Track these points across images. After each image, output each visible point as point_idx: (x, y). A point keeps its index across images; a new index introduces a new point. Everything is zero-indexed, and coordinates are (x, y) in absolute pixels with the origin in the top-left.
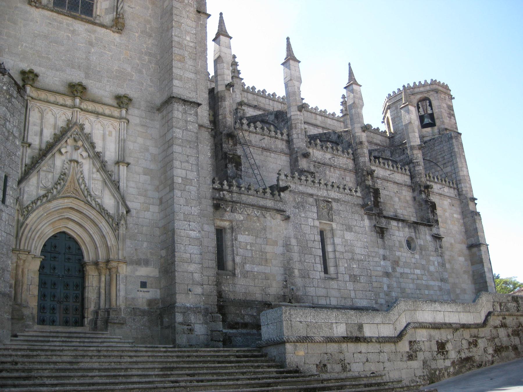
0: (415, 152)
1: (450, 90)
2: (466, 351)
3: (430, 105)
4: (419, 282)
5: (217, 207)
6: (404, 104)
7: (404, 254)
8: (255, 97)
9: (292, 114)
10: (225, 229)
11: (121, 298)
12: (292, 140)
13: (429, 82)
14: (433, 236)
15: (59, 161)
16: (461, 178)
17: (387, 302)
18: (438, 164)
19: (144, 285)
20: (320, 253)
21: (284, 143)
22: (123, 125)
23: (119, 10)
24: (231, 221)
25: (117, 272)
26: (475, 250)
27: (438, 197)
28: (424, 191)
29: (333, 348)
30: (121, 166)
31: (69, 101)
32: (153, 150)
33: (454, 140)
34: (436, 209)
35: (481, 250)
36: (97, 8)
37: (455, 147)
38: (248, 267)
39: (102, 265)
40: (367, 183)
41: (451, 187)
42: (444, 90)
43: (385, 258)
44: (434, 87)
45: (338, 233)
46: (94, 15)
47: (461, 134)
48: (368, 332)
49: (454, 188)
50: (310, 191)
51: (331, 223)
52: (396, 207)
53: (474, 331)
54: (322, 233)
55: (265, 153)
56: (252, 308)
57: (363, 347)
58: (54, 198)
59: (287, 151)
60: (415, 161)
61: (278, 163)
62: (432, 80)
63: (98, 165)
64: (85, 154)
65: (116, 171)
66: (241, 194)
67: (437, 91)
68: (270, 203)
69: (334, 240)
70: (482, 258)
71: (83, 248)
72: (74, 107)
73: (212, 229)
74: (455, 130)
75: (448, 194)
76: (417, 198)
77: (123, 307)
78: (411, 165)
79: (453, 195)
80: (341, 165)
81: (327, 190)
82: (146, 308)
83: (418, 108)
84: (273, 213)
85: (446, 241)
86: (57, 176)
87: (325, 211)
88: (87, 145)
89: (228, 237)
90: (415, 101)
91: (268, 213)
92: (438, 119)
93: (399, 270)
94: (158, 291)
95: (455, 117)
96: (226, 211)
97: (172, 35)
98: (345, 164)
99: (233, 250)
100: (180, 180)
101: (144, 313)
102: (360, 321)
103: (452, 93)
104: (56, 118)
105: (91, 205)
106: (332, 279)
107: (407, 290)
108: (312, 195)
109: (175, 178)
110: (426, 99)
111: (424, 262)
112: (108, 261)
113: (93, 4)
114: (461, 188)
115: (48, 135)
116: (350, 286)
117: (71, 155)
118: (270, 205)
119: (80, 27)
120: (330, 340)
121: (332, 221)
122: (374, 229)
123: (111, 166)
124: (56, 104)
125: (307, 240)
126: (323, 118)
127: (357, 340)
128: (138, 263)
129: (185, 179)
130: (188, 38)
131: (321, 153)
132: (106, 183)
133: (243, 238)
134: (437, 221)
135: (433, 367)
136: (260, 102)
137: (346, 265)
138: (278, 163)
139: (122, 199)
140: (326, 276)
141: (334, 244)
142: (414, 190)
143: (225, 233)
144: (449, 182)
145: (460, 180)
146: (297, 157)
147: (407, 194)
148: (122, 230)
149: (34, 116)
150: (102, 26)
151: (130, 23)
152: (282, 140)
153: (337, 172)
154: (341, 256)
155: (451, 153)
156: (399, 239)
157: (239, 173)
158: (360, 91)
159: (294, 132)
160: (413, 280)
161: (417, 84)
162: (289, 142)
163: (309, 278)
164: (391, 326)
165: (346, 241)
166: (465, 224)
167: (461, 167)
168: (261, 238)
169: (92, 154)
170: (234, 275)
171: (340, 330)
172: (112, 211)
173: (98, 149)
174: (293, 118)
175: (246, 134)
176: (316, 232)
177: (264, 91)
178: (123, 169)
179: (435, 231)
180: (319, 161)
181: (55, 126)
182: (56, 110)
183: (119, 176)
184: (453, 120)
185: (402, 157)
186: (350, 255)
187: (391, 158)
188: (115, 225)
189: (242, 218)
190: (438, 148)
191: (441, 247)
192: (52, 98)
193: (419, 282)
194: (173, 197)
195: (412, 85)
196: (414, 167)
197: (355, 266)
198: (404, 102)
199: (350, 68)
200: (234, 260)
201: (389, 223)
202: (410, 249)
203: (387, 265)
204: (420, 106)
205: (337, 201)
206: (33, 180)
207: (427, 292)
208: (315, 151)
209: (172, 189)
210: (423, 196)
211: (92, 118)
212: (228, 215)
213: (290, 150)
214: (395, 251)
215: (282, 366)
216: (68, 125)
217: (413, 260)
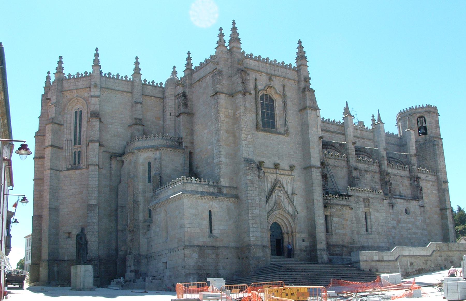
0: (413, 158)
1: (438, 110)
2: (422, 266)
3: (425, 121)
4: (410, 231)
6: (408, 129)
7: (404, 217)
8: (324, 124)
9: (349, 146)
10: (328, 215)
11: (297, 246)
12: (349, 161)
13: (425, 106)
14: (419, 206)
15: (274, 195)
16: (439, 170)
17: (393, 241)
18: (427, 159)
19: (303, 241)
21: (345, 162)
23: (287, 125)
24: (331, 213)
25: (295, 236)
26: (443, 211)
27: (424, 182)
28: (416, 181)
29: (374, 264)
30: (294, 196)
32: (303, 187)
33: (436, 147)
34: (422, 190)
35: (447, 212)
36: (277, 124)
37: (437, 150)
38: (337, 231)
39: (290, 234)
40: (386, 180)
41: (433, 175)
42: (434, 110)
43: (393, 219)
44: (428, 109)
45: (372, 213)
46: (276, 128)
47: (442, 139)
48: (385, 258)
49: (435, 176)
50: (360, 195)
51: (369, 209)
52: (401, 190)
53: (426, 258)
55: (336, 169)
56: (339, 247)
58: (274, 210)
59: (347, 167)
60: (412, 163)
61: (343, 173)
62: (427, 105)
63: (287, 196)
64: (282, 192)
65: (292, 197)
66: (334, 200)
67: (429, 112)
68: (345, 203)
69: (370, 217)
70: (447, 216)
71: (282, 228)
73: (325, 216)
74: (439, 136)
75: (431, 180)
76: (412, 184)
77: (298, 249)
78: (410, 165)
79: (434, 180)
80: (373, 170)
81: (368, 194)
82: (305, 249)
83: (418, 122)
84: (346, 207)
85: (428, 207)
86: (274, 202)
87: (367, 204)
88: (282, 189)
89: (329, 219)
90: (416, 118)
91: (344, 207)
92: (429, 130)
93: (400, 225)
94: (308, 243)
95: (439, 128)
96: (328, 208)
97: (309, 137)
98: (375, 169)
99: (331, 224)
100: (316, 200)
101: (305, 251)
102: (382, 255)
103: (438, 112)
104: (271, 179)
105: (286, 212)
106: (369, 234)
107: (404, 235)
108: (362, 197)
109: (314, 200)
110: (422, 117)
111: (413, 221)
112: (292, 232)
113: (275, 122)
114: (439, 175)
116: (377, 237)
117: (278, 193)
118: (345, 204)
119: (274, 136)
120: (373, 261)
121: (370, 208)
122: (388, 204)
123: (290, 196)
124: (270, 173)
125: (359, 218)
126: (361, 131)
128: (301, 232)
129: (318, 200)
130: (315, 138)
131: (363, 165)
132: (289, 203)
133: (335, 219)
134: (422, 198)
135: (408, 271)
136: (327, 127)
137: (375, 228)
138: (343, 173)
140: (368, 233)
141: (370, 218)
142: (411, 180)
143: (328, 217)
144: (432, 172)
145: (438, 171)
146: (352, 170)
147: (407, 182)
148: (296, 221)
150: (280, 134)
151: (291, 130)
152: (344, 160)
153: (371, 174)
154: (374, 224)
155: (435, 154)
156: (401, 209)
157: (326, 182)
158: (384, 127)
159: (350, 157)
160: (407, 230)
161: (418, 107)
162: (348, 161)
163: (360, 234)
164: (393, 257)
165: (376, 216)
166: (439, 197)
167: (439, 163)
168: (341, 218)
169: (284, 192)
170: (332, 234)
171: (376, 258)
173: (286, 190)
174: (349, 149)
175: (328, 160)
176: (363, 214)
177: (329, 120)
178: (295, 197)
179: (421, 203)
180: (362, 169)
181: (271, 182)
182: (271, 175)
183: (293, 199)
184: (438, 130)
185: (405, 160)
186: (377, 223)
187: (399, 159)
189: (334, 210)
190: (427, 149)
191: (424, 212)
193: (410, 231)
194: (314, 208)
195: (414, 107)
196: (412, 166)
197: (379, 228)
198: (408, 128)
199: (378, 112)
200: (332, 229)
201: (396, 201)
202: (406, 214)
203: (394, 223)
204: (419, 121)
205: (373, 198)
206: (268, 203)
207: (414, 236)
208: (359, 164)
209: (314, 205)
210: (416, 183)
211: (282, 177)
212: (329, 210)
213: (348, 165)
214: (398, 215)
215: (360, 269)
216: (275, 182)
217: (408, 220)
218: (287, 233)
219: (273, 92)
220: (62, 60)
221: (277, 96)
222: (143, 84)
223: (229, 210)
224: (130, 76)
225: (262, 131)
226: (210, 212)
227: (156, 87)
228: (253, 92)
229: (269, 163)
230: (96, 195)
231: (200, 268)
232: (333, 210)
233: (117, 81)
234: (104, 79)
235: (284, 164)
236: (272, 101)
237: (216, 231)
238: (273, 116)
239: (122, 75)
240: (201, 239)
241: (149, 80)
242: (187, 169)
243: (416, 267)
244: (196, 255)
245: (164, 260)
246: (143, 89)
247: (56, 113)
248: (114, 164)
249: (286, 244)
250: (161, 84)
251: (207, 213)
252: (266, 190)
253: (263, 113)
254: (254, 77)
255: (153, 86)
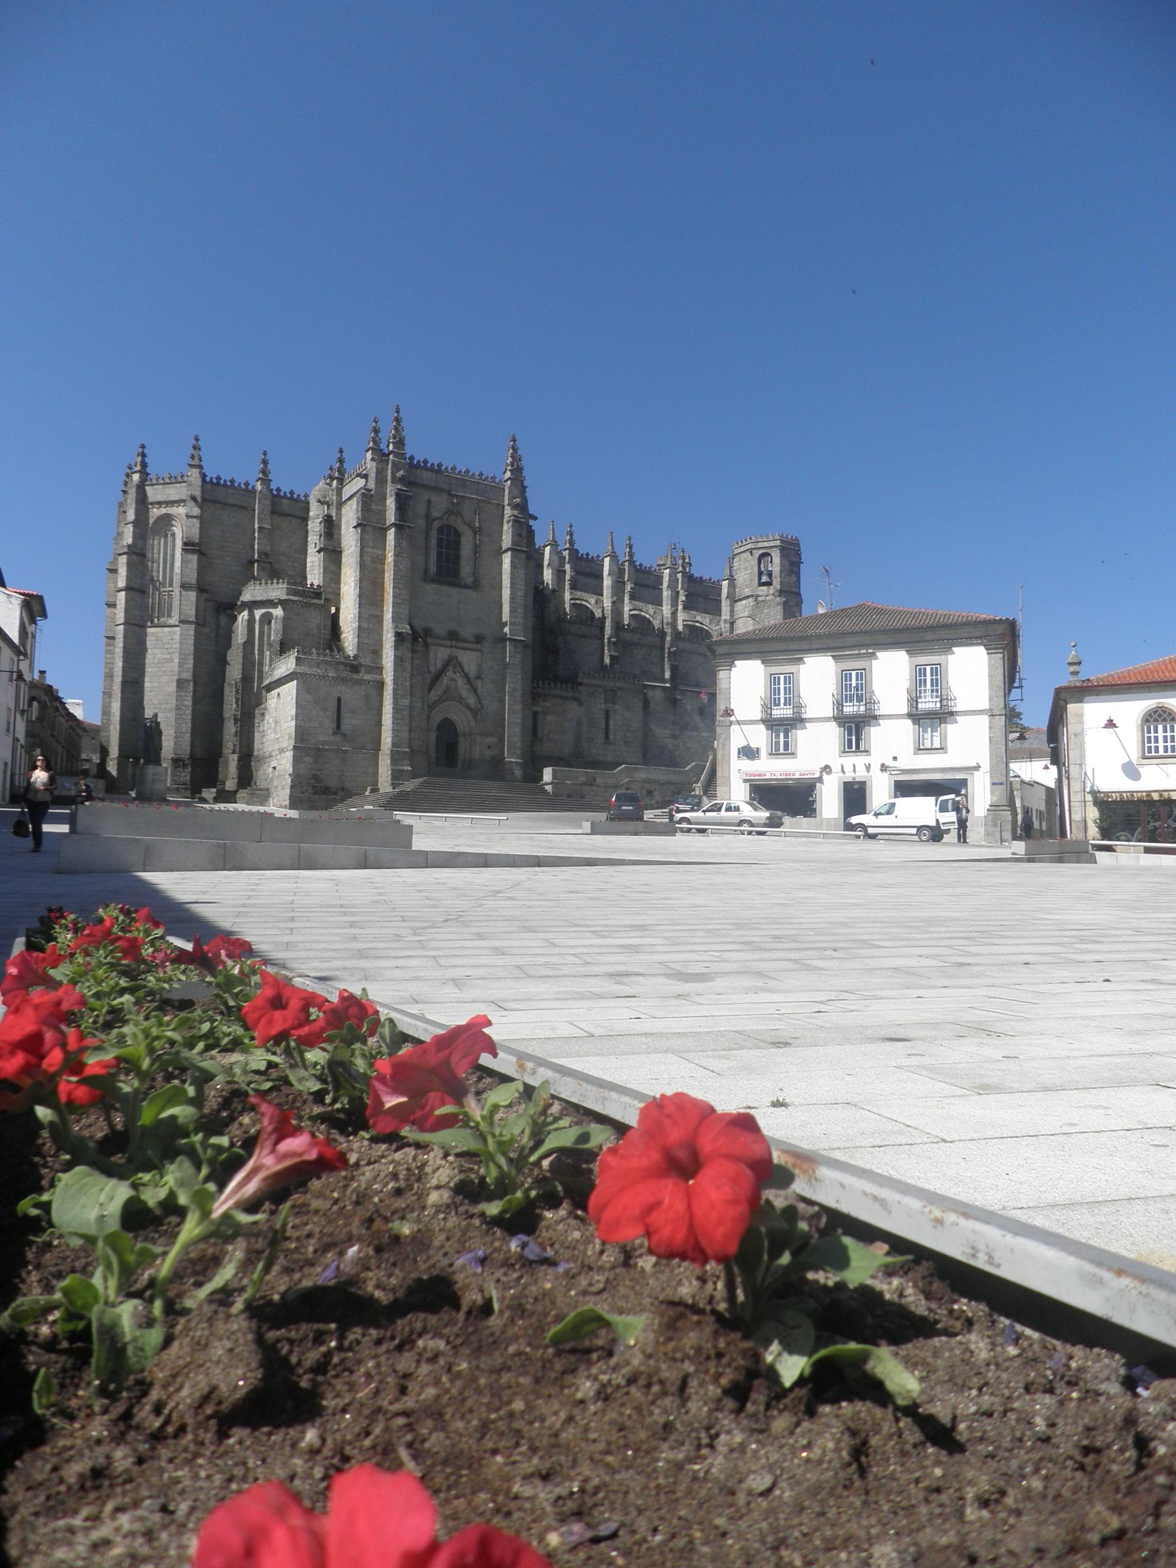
5: (534, 699)
15: (445, 680)
20: (604, 726)
22: (479, 654)
31: (449, 643)
50: (600, 683)
54: (607, 713)
57: (595, 788)
68: (570, 694)
72: (451, 646)
83: (759, 563)
115: (439, 664)
119: (454, 591)
124: (443, 645)
127: (591, 785)
133: (549, 718)
139: (479, 699)
149: (432, 654)
150: (466, 587)
172: (473, 706)
178: (479, 683)
182: (441, 649)
188: (475, 712)
192: (441, 642)
205: (621, 689)
206: (433, 692)
211: (461, 652)
218: (464, 735)
219: (460, 521)
220: (146, 451)
221: (466, 528)
222: (274, 496)
223: (367, 697)
224: (252, 483)
225: (433, 581)
226: (339, 699)
227: (297, 500)
228: (421, 523)
229: (440, 629)
230: (191, 666)
231: (315, 777)
232: (548, 704)
233: (230, 491)
234: (209, 486)
235: (467, 632)
236: (458, 535)
237: (344, 727)
238: (457, 559)
239: (240, 480)
240: (321, 738)
241: (285, 489)
242: (327, 633)
243: (658, 798)
244: (309, 760)
245: (273, 764)
246: (273, 503)
247: (134, 537)
248: (223, 619)
249: (462, 749)
250: (306, 496)
251: (332, 704)
252: (433, 669)
253: (439, 554)
254: (427, 497)
255: (291, 499)
